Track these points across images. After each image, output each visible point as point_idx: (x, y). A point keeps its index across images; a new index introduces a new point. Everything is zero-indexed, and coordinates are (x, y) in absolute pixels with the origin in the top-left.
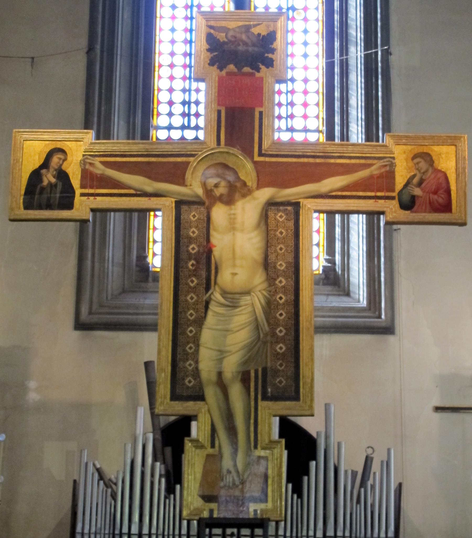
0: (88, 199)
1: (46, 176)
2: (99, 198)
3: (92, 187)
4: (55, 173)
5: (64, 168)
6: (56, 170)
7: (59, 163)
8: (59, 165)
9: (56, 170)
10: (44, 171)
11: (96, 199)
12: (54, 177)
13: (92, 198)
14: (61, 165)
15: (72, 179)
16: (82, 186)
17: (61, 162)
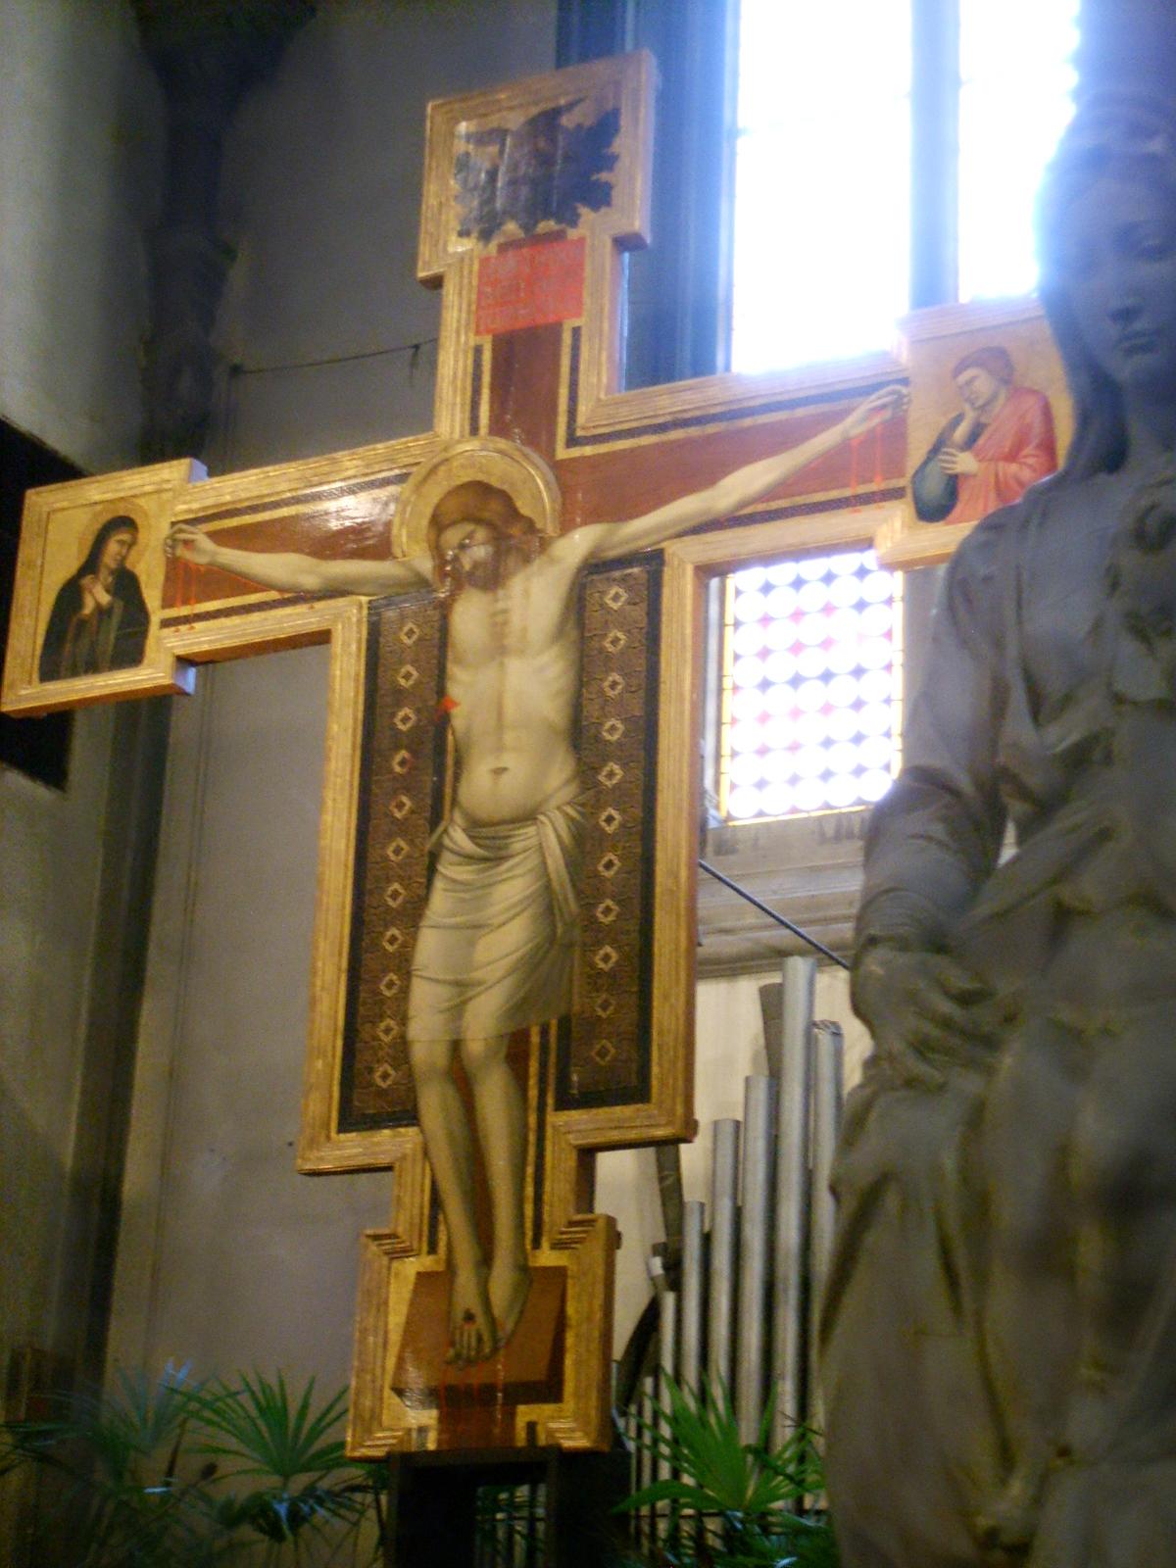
0: (177, 631)
1: (91, 592)
2: (199, 626)
3: (186, 602)
4: (110, 579)
5: (128, 565)
6: (112, 572)
7: (119, 554)
8: (119, 558)
9: (112, 572)
10: (86, 581)
11: (192, 628)
12: (108, 591)
13: (183, 628)
14: (124, 558)
15: (146, 587)
16: (167, 603)
17: (124, 551)
